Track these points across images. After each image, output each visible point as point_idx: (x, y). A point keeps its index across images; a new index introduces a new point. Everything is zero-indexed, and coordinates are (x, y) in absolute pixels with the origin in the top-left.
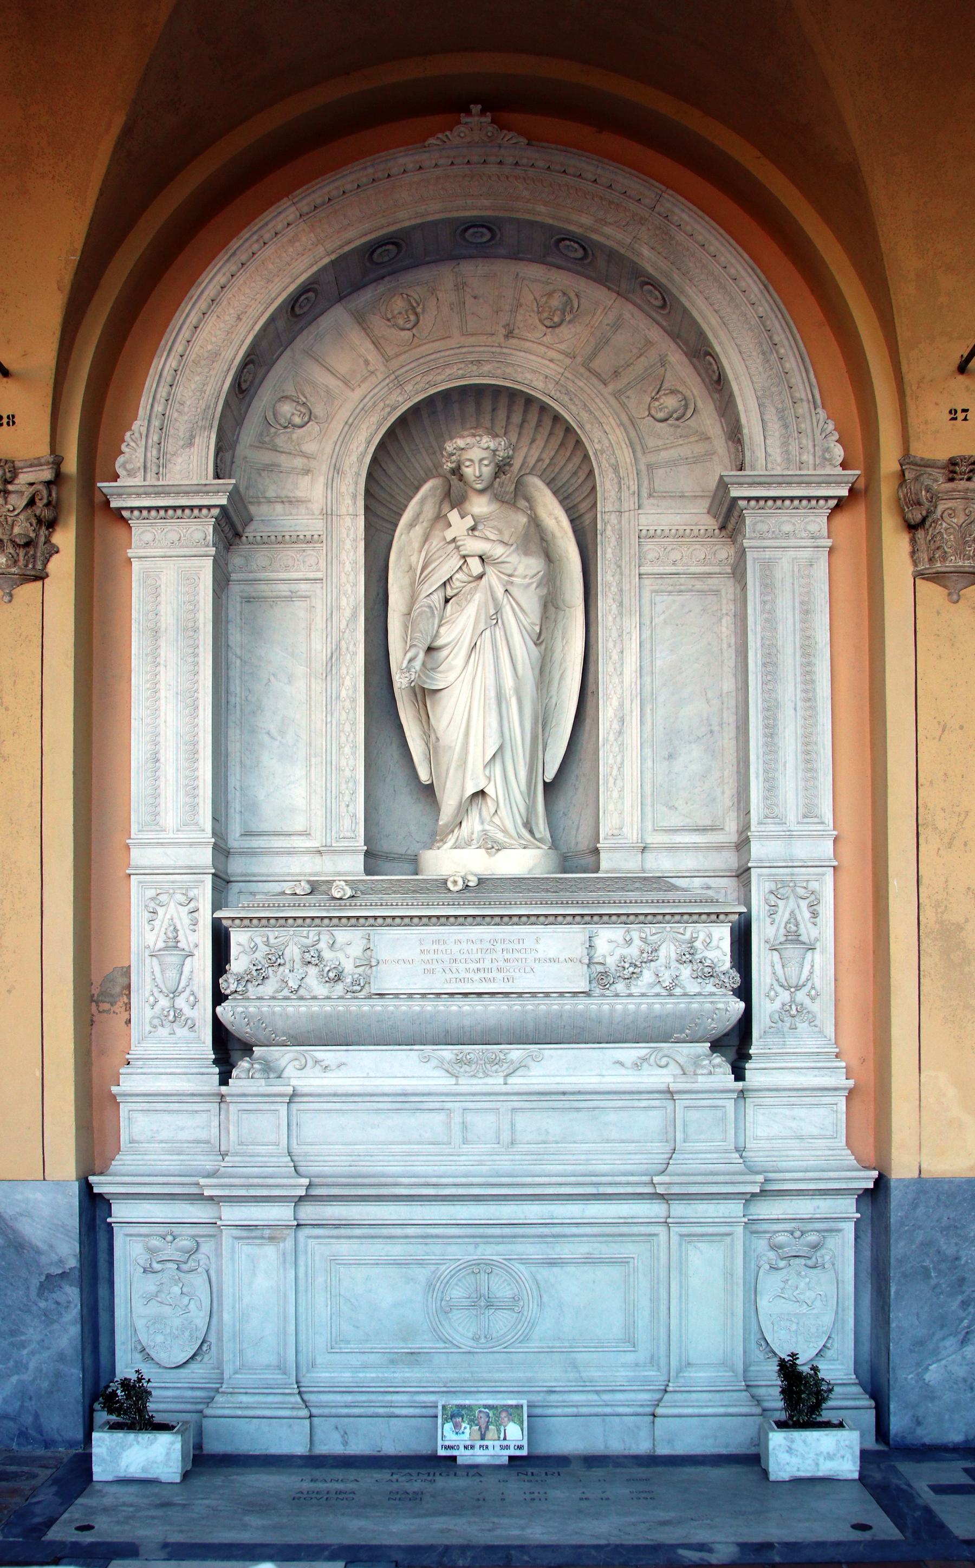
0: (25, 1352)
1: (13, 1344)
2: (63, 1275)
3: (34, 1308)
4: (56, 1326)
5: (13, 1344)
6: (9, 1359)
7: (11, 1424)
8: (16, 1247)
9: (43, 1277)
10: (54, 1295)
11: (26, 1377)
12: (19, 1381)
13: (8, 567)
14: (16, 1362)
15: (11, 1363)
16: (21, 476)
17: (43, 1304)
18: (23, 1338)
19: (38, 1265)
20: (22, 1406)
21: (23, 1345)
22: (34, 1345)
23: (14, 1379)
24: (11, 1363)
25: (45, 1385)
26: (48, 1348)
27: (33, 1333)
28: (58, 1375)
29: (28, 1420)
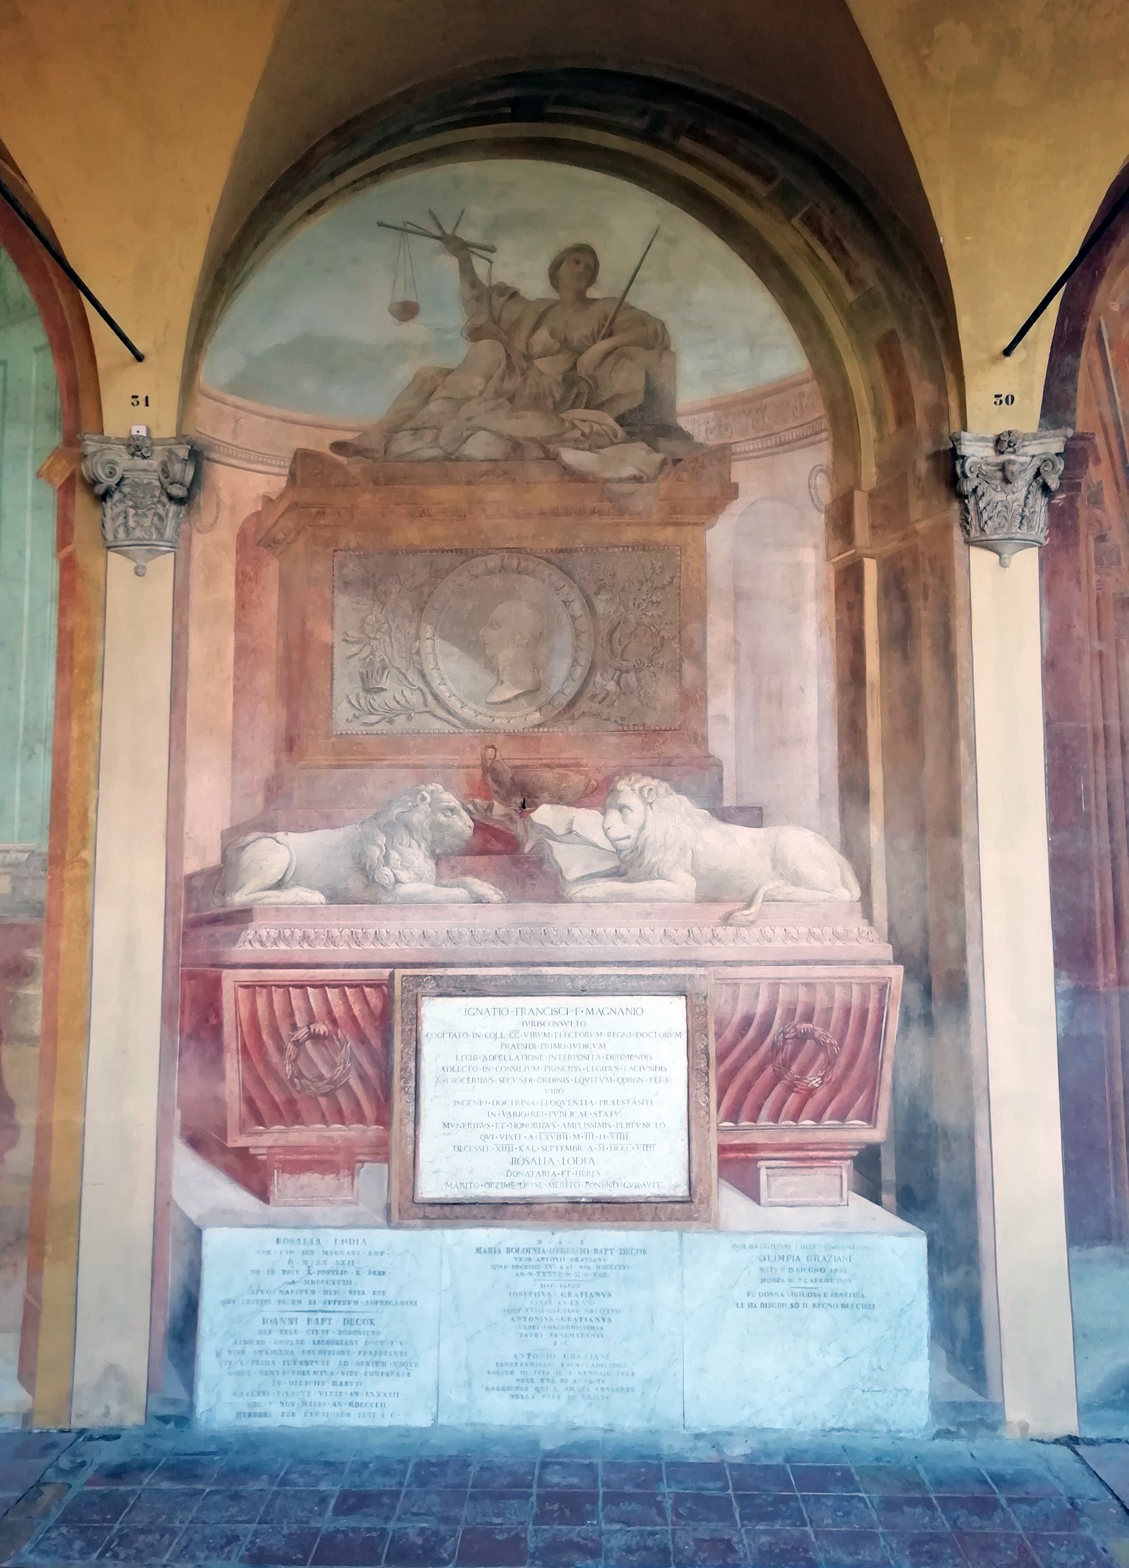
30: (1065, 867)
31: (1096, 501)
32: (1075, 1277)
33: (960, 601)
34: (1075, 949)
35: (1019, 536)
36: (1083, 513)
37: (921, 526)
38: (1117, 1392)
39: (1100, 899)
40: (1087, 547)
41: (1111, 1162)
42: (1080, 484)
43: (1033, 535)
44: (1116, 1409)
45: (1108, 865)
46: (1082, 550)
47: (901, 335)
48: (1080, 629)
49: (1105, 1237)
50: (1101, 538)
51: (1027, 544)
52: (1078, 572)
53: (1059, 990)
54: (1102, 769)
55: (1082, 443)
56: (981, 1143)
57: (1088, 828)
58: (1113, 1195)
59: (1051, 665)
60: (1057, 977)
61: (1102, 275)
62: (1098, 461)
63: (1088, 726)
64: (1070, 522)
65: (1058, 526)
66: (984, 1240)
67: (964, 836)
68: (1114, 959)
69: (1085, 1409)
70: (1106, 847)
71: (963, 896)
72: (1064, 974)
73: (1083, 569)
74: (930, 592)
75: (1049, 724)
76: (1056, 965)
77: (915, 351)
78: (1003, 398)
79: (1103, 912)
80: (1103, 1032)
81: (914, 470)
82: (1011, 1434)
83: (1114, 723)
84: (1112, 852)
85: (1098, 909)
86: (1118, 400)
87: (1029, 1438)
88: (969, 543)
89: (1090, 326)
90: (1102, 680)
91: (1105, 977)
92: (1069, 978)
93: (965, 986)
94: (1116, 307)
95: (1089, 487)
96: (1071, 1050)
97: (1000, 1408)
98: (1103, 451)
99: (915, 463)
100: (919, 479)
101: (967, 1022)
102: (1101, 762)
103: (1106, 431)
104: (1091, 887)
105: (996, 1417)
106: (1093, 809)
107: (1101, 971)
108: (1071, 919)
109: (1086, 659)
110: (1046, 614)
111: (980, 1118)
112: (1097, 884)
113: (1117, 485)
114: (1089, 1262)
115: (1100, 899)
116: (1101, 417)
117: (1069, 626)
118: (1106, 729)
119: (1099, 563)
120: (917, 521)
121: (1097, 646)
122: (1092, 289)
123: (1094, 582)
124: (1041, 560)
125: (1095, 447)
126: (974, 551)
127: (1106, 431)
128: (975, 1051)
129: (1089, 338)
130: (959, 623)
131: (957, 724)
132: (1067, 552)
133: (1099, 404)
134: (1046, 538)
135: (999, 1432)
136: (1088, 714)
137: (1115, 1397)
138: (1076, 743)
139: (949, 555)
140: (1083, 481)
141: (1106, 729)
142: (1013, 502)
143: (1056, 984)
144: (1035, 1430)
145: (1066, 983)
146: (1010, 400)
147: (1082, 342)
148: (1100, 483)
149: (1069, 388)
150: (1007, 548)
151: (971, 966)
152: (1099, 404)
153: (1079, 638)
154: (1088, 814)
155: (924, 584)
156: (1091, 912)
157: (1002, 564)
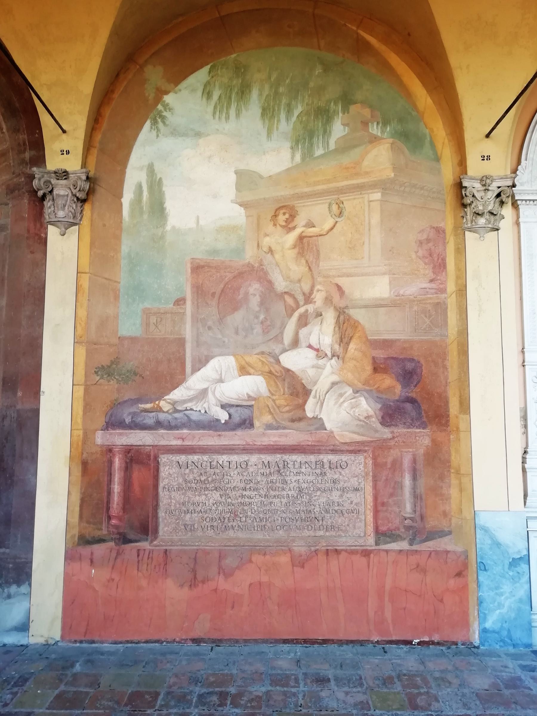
0: (503, 598)
1: (497, 594)
2: (521, 558)
3: (507, 576)
4: (518, 585)
5: (497, 594)
6: (495, 602)
7: (496, 635)
8: (497, 544)
9: (511, 560)
10: (516, 569)
11: (504, 610)
12: (500, 613)
13: (485, 224)
14: (498, 603)
15: (496, 604)
16: (493, 183)
17: (511, 573)
18: (502, 590)
19: (508, 553)
20: (502, 626)
21: (502, 594)
22: (507, 594)
23: (498, 612)
24: (496, 604)
25: (513, 615)
26: (514, 596)
27: (506, 588)
28: (519, 610)
29: (505, 633)
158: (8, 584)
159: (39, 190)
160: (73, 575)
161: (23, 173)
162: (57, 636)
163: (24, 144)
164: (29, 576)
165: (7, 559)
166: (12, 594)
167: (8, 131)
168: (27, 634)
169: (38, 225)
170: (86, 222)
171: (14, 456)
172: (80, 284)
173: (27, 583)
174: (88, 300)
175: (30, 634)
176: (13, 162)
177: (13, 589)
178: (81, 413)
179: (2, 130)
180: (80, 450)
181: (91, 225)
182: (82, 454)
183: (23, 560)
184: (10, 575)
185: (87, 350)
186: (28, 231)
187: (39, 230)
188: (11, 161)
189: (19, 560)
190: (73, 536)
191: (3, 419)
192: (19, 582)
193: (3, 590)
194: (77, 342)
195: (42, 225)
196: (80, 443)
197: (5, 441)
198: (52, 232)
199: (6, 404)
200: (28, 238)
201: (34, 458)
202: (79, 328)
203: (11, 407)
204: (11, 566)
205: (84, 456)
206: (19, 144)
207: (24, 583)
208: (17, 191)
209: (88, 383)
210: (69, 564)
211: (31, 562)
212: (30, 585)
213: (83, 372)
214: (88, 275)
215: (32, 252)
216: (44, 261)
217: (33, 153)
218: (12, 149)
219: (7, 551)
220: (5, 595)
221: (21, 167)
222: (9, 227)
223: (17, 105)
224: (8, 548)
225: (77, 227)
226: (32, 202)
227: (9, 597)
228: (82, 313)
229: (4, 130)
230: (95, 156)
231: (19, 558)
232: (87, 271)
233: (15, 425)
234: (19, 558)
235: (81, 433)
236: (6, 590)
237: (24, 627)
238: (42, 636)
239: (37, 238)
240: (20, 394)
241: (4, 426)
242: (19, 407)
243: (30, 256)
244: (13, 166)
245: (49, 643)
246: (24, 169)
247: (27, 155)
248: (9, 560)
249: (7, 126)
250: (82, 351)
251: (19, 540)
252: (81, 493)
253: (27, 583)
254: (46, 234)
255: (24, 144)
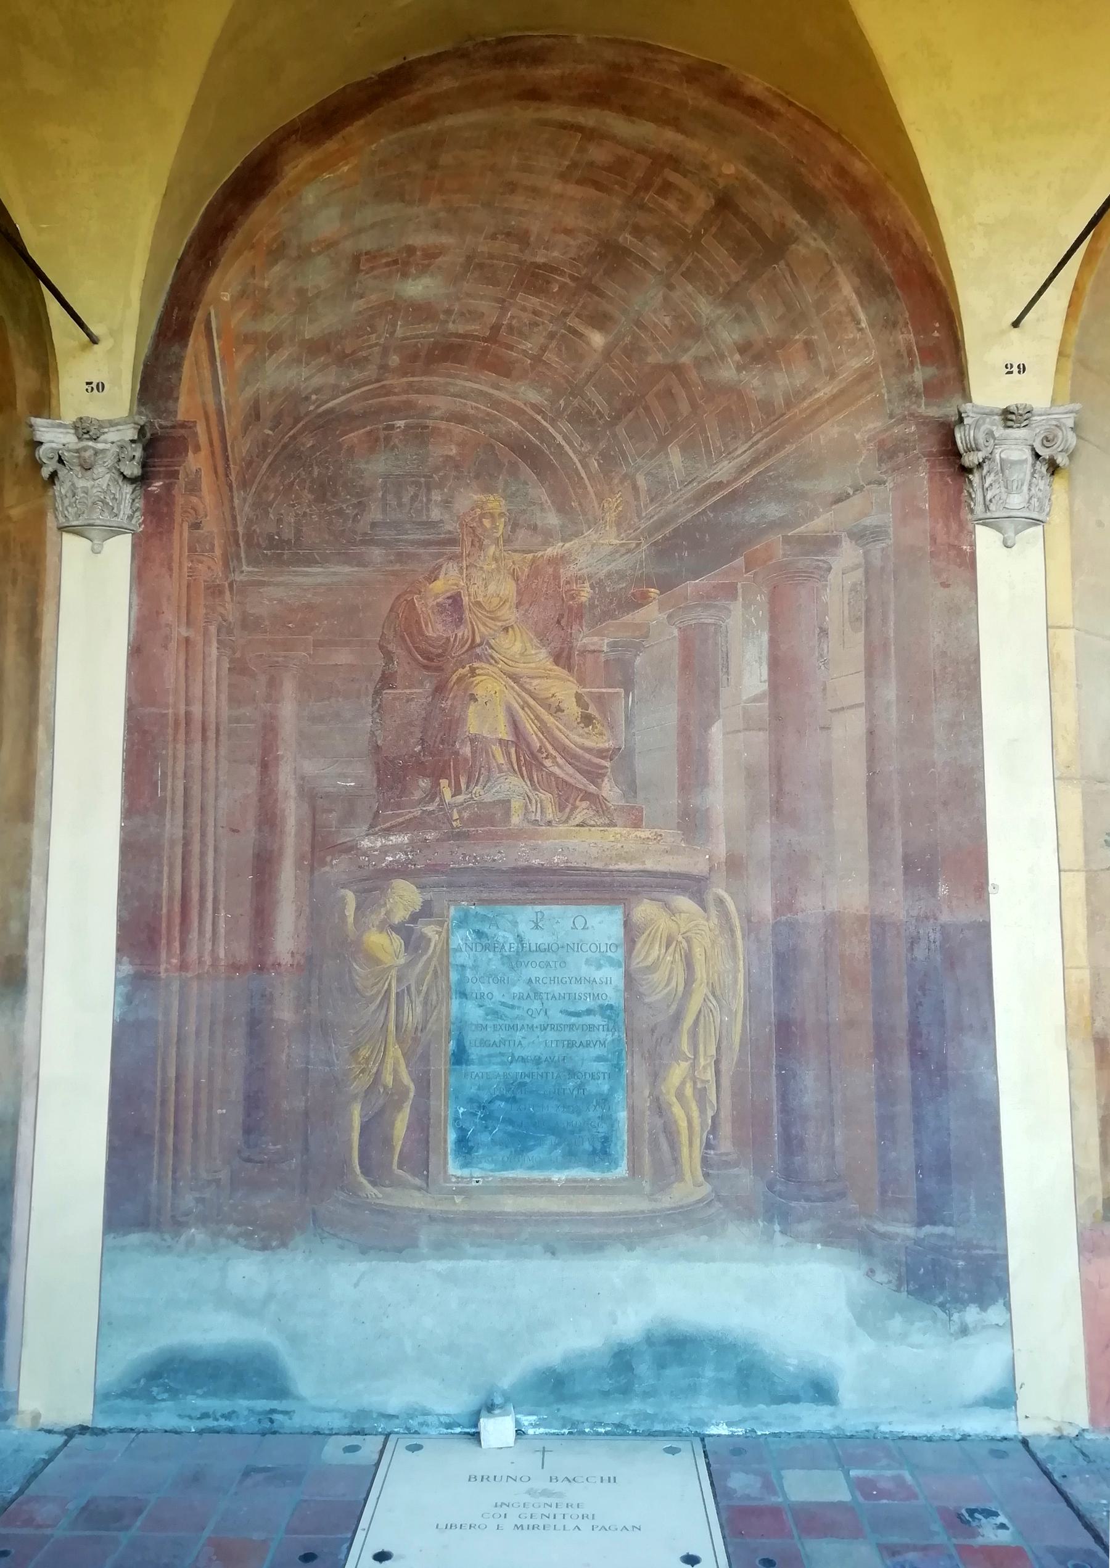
30: (135, 852)
31: (193, 488)
32: (106, 1266)
33: (49, 587)
34: (141, 933)
35: (98, 522)
36: (180, 501)
37: (15, 513)
38: (138, 1381)
39: (169, 885)
40: (181, 534)
41: (156, 1149)
42: (177, 472)
43: (122, 519)
44: (134, 1398)
45: (179, 850)
46: (176, 536)
47: (9, 324)
48: (169, 616)
49: (143, 1223)
50: (196, 526)
51: (115, 531)
52: (171, 558)
53: (121, 975)
54: (181, 755)
55: (182, 431)
56: (25, 1130)
57: (161, 813)
58: (155, 1182)
59: (136, 651)
60: (118, 962)
61: (215, 266)
62: (197, 449)
63: (171, 711)
64: (165, 510)
65: (153, 514)
66: (18, 1228)
67: (36, 821)
68: (177, 944)
69: (102, 1398)
70: (179, 833)
71: (30, 881)
72: (125, 959)
73: (176, 557)
74: (20, 578)
75: (131, 709)
76: (118, 950)
77: (22, 338)
78: (94, 385)
79: (171, 899)
80: (160, 1018)
81: (11, 456)
82: (20, 1424)
83: (196, 710)
84: (184, 838)
85: (165, 894)
86: (222, 389)
87: (39, 1427)
88: (62, 529)
89: (200, 315)
90: (187, 667)
91: (166, 964)
92: (131, 963)
93: (24, 972)
94: (226, 297)
95: (187, 475)
96: (125, 1035)
97: (14, 1397)
98: (203, 439)
99: (13, 450)
100: (17, 466)
101: (22, 1009)
102: (181, 747)
103: (207, 419)
104: (161, 872)
105: (8, 1406)
106: (169, 794)
107: (163, 955)
108: (137, 904)
109: (173, 645)
110: (135, 601)
111: (27, 1106)
112: (166, 869)
113: (216, 472)
114: (123, 1248)
115: (169, 885)
116: (204, 405)
117: (158, 613)
118: (188, 714)
119: (192, 549)
120: (11, 507)
121: (184, 633)
122: (204, 278)
123: (186, 570)
124: (134, 546)
125: (196, 434)
126: (66, 537)
127: (207, 419)
128: (28, 1038)
129: (197, 327)
130: (47, 609)
131: (37, 708)
132: (161, 540)
133: (202, 393)
134: (140, 525)
135: (10, 1422)
136: (171, 700)
137: (135, 1386)
138: (156, 730)
139: (40, 540)
140: (181, 469)
141: (188, 714)
142: (101, 488)
143: (117, 970)
144: (46, 1421)
145: (127, 969)
146: (101, 387)
147: (191, 331)
148: (198, 471)
149: (173, 376)
150: (94, 533)
151: (31, 952)
152: (202, 393)
153: (167, 625)
154: (163, 800)
155: (14, 570)
156: (158, 897)
157: (95, 552)
158: (960, 1303)
159: (970, 450)
160: (1101, 1287)
161: (912, 415)
162: (1082, 1420)
163: (910, 353)
164: (1003, 1287)
165: (951, 1249)
166: (970, 1326)
167: (872, 325)
168: (1013, 1414)
169: (954, 527)
170: (1058, 517)
171: (942, 1024)
172: (1054, 651)
173: (1001, 1301)
174: (1077, 685)
175: (1021, 1413)
176: (889, 392)
177: (972, 1314)
178: (1082, 930)
179: (859, 323)
180: (1087, 1014)
181: (1072, 525)
182: (1093, 1020)
183: (986, 1252)
184: (963, 1285)
185: (1085, 795)
186: (934, 539)
187: (957, 537)
188: (884, 391)
189: (978, 1252)
190: (1092, 1200)
191: (912, 943)
192: (983, 1301)
193: (950, 1316)
194: (1060, 778)
195: (962, 525)
196: (1086, 998)
197: (919, 993)
198: (985, 540)
199: (915, 913)
200: (932, 554)
201: (986, 1029)
202: (1062, 749)
203: (927, 918)
204: (961, 1263)
205: (1099, 1023)
206: (899, 355)
207: (994, 1301)
208: (901, 455)
209: (1094, 867)
210: (1089, 1261)
211: (1005, 1257)
212: (1008, 1306)
213: (1080, 844)
214: (1072, 632)
215: (945, 585)
216: (972, 604)
217: (931, 371)
218: (884, 364)
219: (950, 1231)
220: (954, 1328)
221: (907, 403)
222: (891, 530)
223: (887, 269)
224: (950, 1225)
225: (1040, 528)
226: (938, 477)
227: (964, 1331)
228: (1067, 714)
229: (864, 325)
230: (1070, 374)
231: (978, 1247)
232: (1070, 623)
233: (939, 958)
234: (978, 1247)
235: (1086, 974)
236: (956, 1316)
237: (1004, 1399)
238: (1048, 1418)
239: (953, 553)
240: (943, 890)
241: (914, 959)
242: (945, 917)
243: (941, 593)
244: (890, 401)
245: (1065, 1433)
246: (914, 407)
247: (918, 376)
248: (955, 1251)
249: (867, 315)
250: (1073, 798)
251: (973, 1208)
252: (1099, 1106)
253: (1001, 1301)
254: (973, 545)
255: (910, 353)
